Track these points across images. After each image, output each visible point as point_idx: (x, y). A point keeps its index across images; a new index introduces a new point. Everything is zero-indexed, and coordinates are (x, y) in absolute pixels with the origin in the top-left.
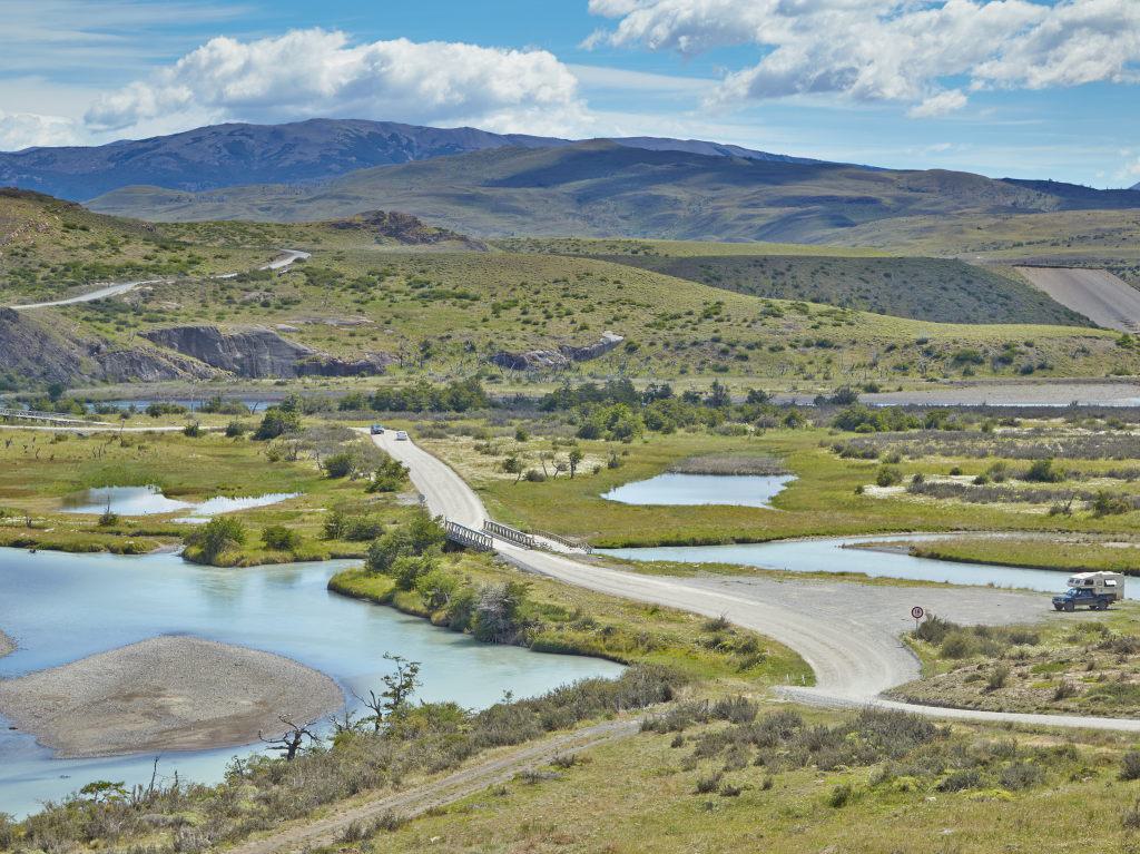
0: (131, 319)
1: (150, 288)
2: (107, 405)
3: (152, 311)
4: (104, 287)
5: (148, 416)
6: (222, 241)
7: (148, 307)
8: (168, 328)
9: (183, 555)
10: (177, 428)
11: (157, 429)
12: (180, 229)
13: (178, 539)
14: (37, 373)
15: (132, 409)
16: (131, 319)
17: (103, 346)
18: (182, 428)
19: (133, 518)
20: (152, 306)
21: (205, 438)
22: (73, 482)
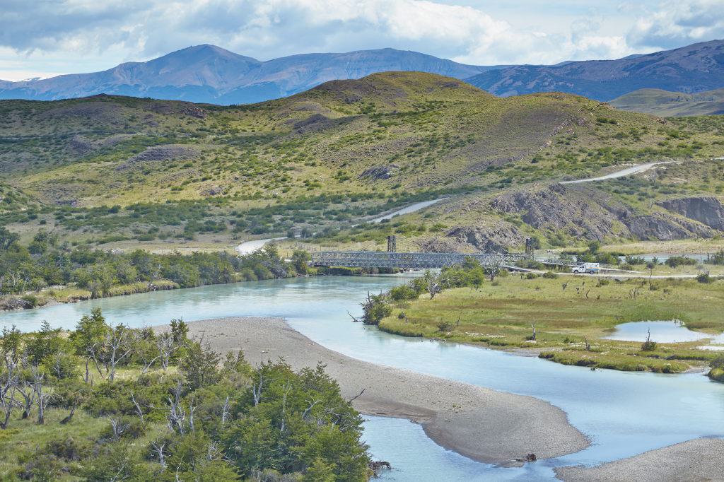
0: (649, 191)
1: (664, 168)
2: (636, 257)
3: (666, 185)
4: (628, 167)
5: (668, 266)
6: (716, 131)
7: (663, 182)
8: (678, 198)
9: (710, 375)
10: (692, 276)
11: (676, 276)
12: (683, 122)
13: (703, 362)
14: (580, 233)
15: (655, 261)
16: (649, 191)
17: (629, 212)
18: (696, 276)
19: (667, 345)
20: (666, 181)
21: (714, 284)
22: (616, 316)
